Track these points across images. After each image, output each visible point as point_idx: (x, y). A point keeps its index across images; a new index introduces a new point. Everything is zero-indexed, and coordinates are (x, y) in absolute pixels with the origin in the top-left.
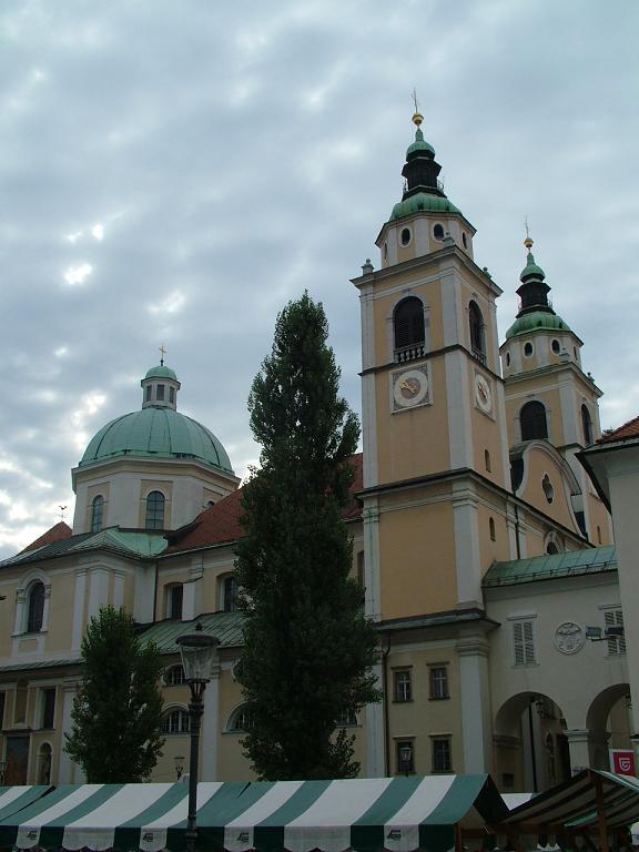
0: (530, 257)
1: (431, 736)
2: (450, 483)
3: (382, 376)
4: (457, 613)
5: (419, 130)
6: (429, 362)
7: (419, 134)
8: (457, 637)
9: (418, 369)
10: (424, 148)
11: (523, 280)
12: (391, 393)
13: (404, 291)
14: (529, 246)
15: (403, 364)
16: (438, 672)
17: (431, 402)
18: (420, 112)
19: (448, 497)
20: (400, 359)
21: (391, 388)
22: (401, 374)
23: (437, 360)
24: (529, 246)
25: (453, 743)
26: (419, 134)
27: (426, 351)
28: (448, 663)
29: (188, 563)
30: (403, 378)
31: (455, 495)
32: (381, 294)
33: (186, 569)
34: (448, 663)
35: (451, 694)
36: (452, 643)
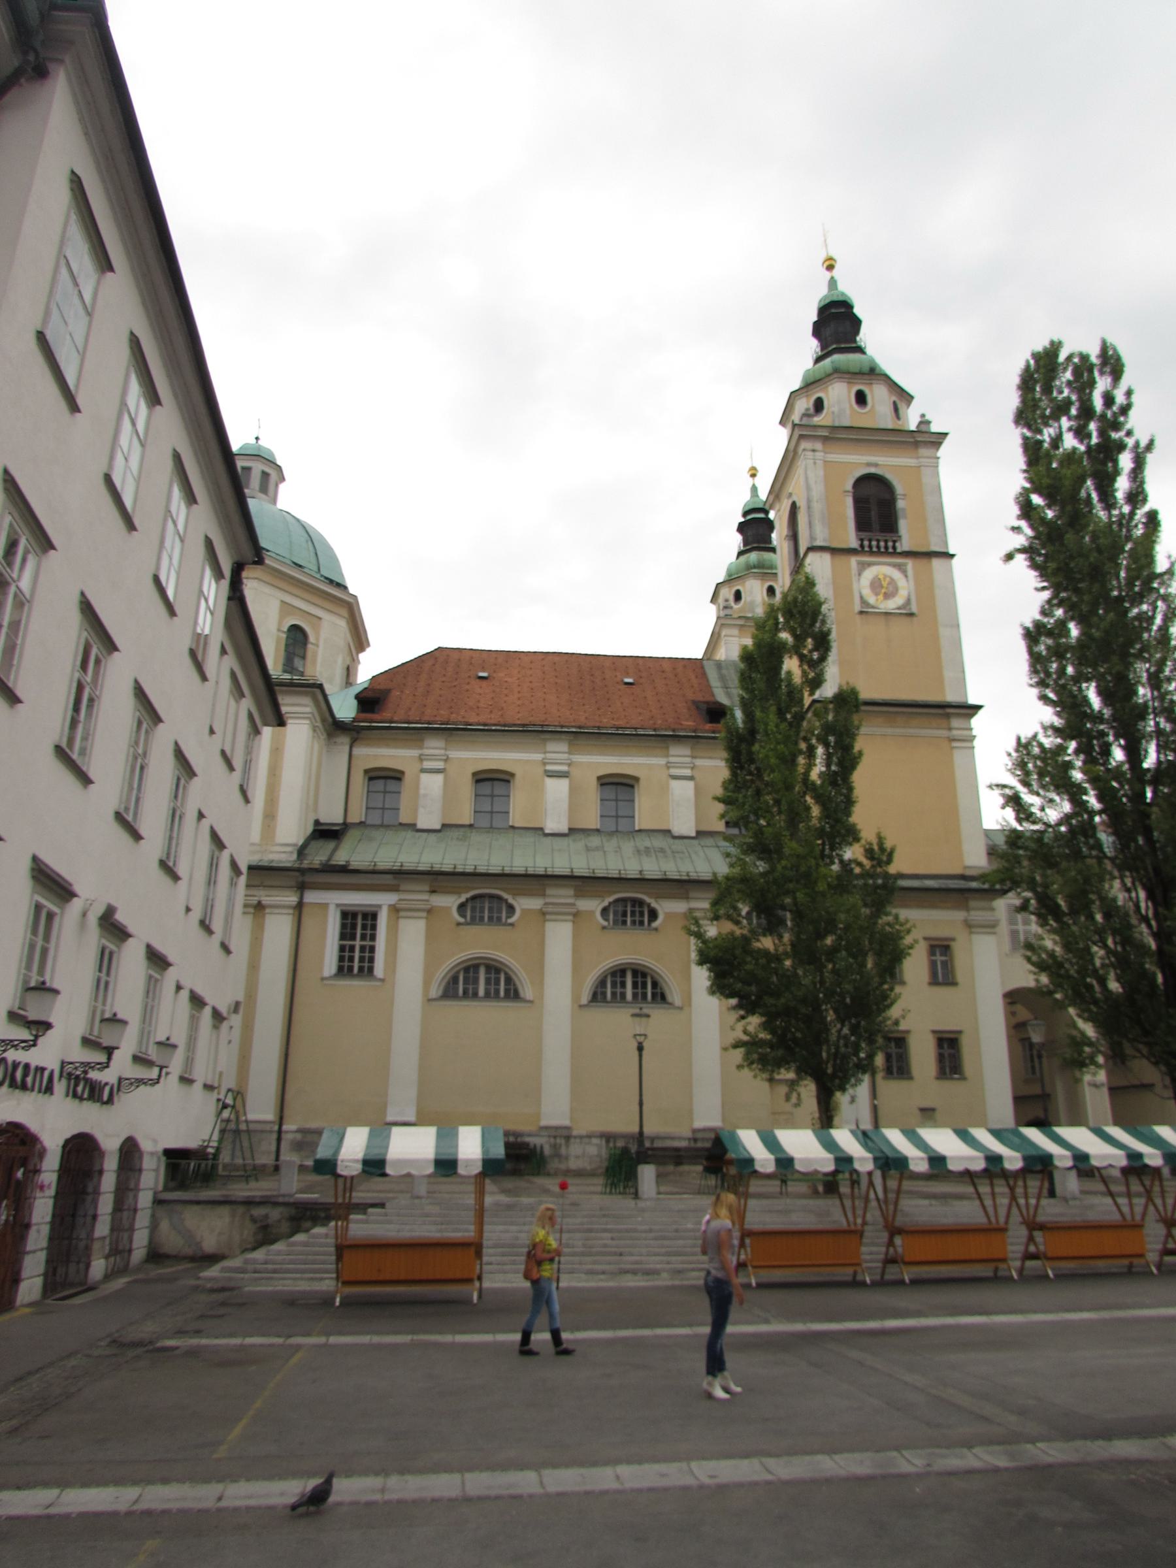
0: (754, 489)
1: (934, 1032)
2: (948, 716)
3: (842, 559)
4: (963, 877)
5: (832, 278)
6: (910, 564)
7: (833, 283)
8: (968, 909)
9: (894, 565)
10: (841, 298)
11: (745, 514)
12: (855, 586)
13: (869, 465)
14: (753, 476)
15: (871, 553)
16: (941, 949)
17: (914, 609)
18: (832, 254)
19: (944, 733)
20: (862, 546)
21: (855, 579)
22: (870, 564)
23: (921, 563)
24: (753, 476)
25: (966, 1044)
26: (833, 283)
27: (905, 545)
28: (953, 939)
29: (419, 743)
30: (869, 574)
31: (955, 733)
32: (832, 457)
33: (415, 753)
34: (953, 939)
35: (960, 977)
36: (960, 915)
